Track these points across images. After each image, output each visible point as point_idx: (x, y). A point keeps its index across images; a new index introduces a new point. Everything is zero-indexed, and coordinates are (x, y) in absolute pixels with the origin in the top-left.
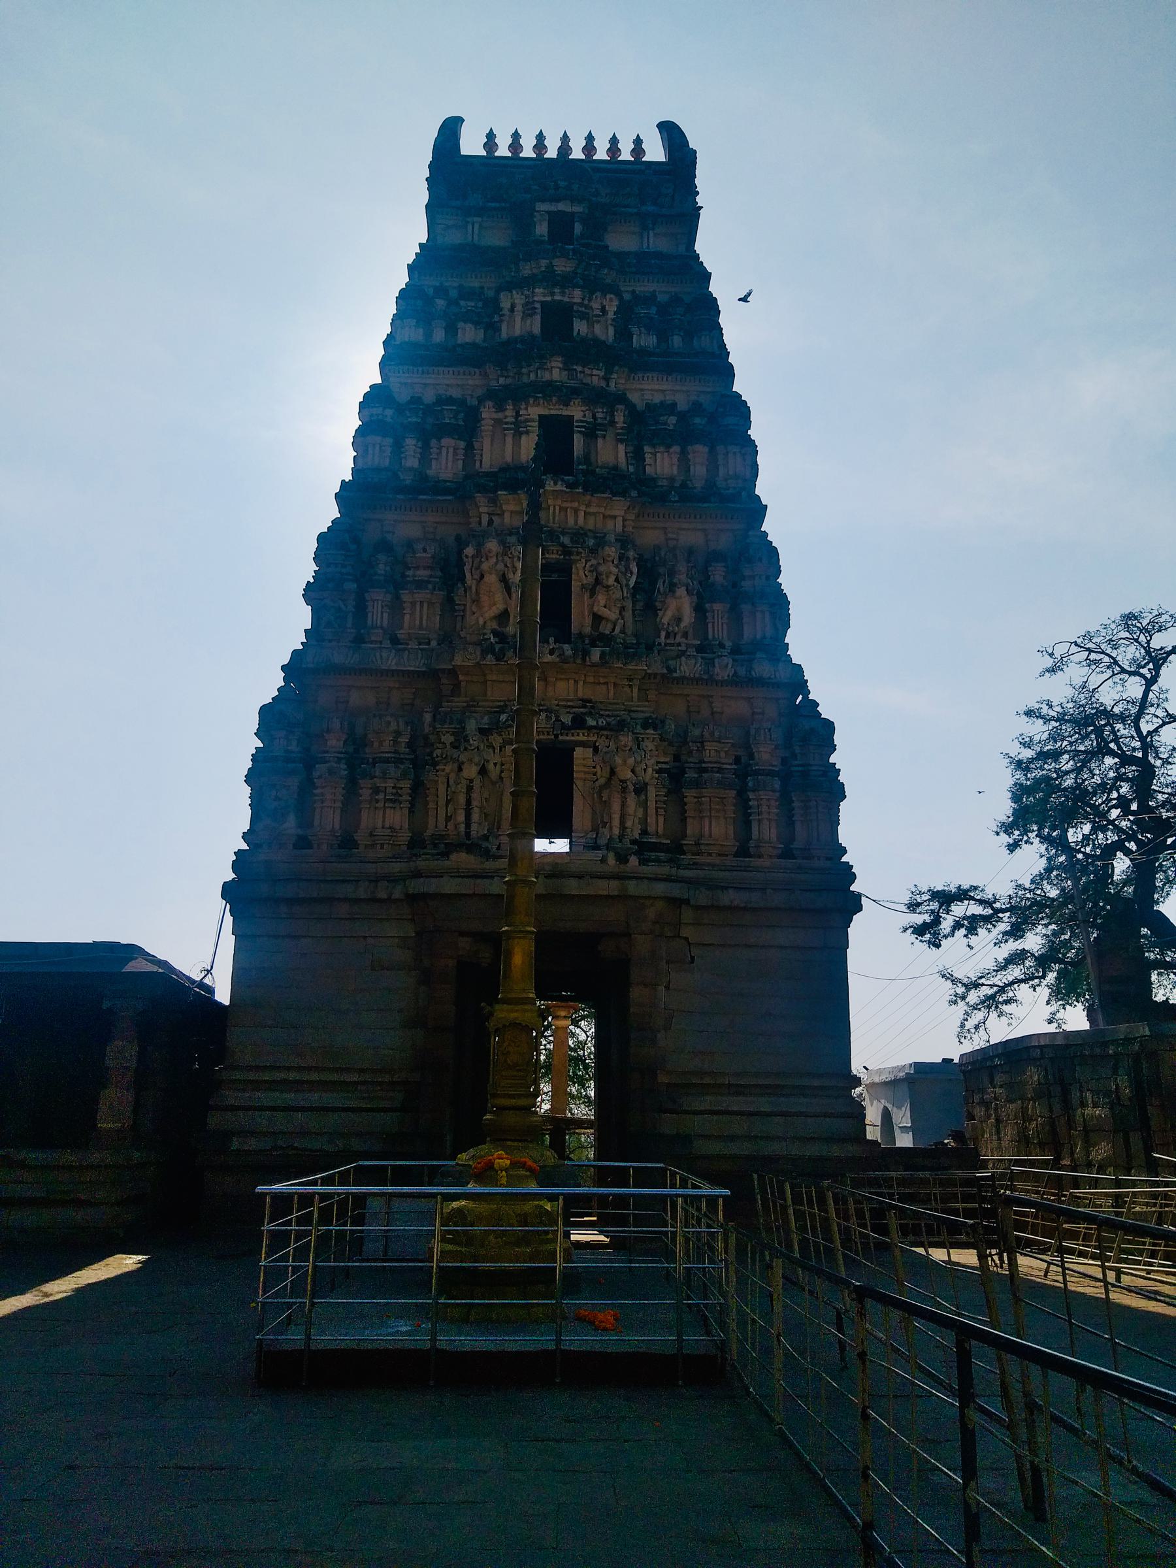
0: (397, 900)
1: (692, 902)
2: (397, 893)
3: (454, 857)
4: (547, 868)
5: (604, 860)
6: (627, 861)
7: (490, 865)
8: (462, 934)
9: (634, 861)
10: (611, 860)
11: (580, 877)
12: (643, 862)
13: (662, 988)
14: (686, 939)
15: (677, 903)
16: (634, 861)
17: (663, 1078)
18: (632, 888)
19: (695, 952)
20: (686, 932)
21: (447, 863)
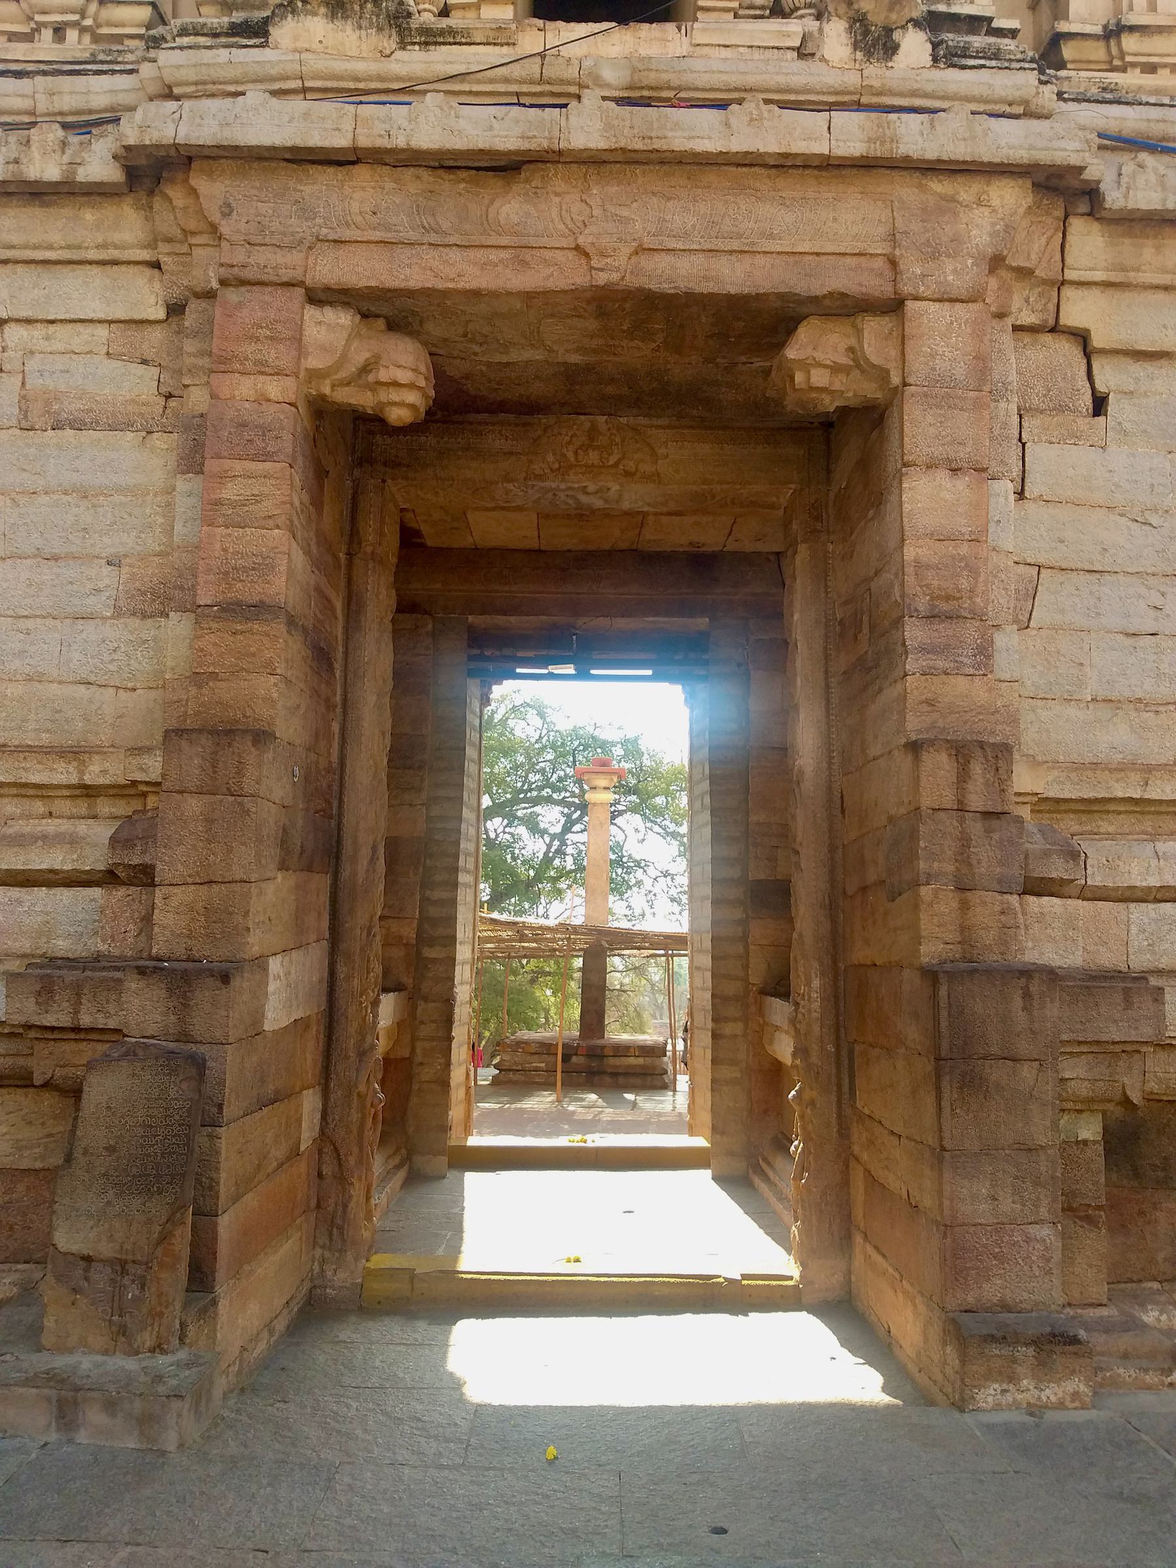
0: (96, 192)
1: (1114, 198)
2: (98, 164)
3: (284, 32)
4: (609, 75)
5: (803, 52)
6: (891, 49)
7: (414, 62)
8: (320, 297)
9: (914, 46)
10: (836, 40)
11: (722, 105)
12: (946, 57)
13: (1006, 487)
14: (1082, 338)
15: (1063, 191)
16: (914, 46)
17: (1024, 780)
18: (913, 137)
19: (1107, 376)
20: (1079, 310)
21: (267, 54)
